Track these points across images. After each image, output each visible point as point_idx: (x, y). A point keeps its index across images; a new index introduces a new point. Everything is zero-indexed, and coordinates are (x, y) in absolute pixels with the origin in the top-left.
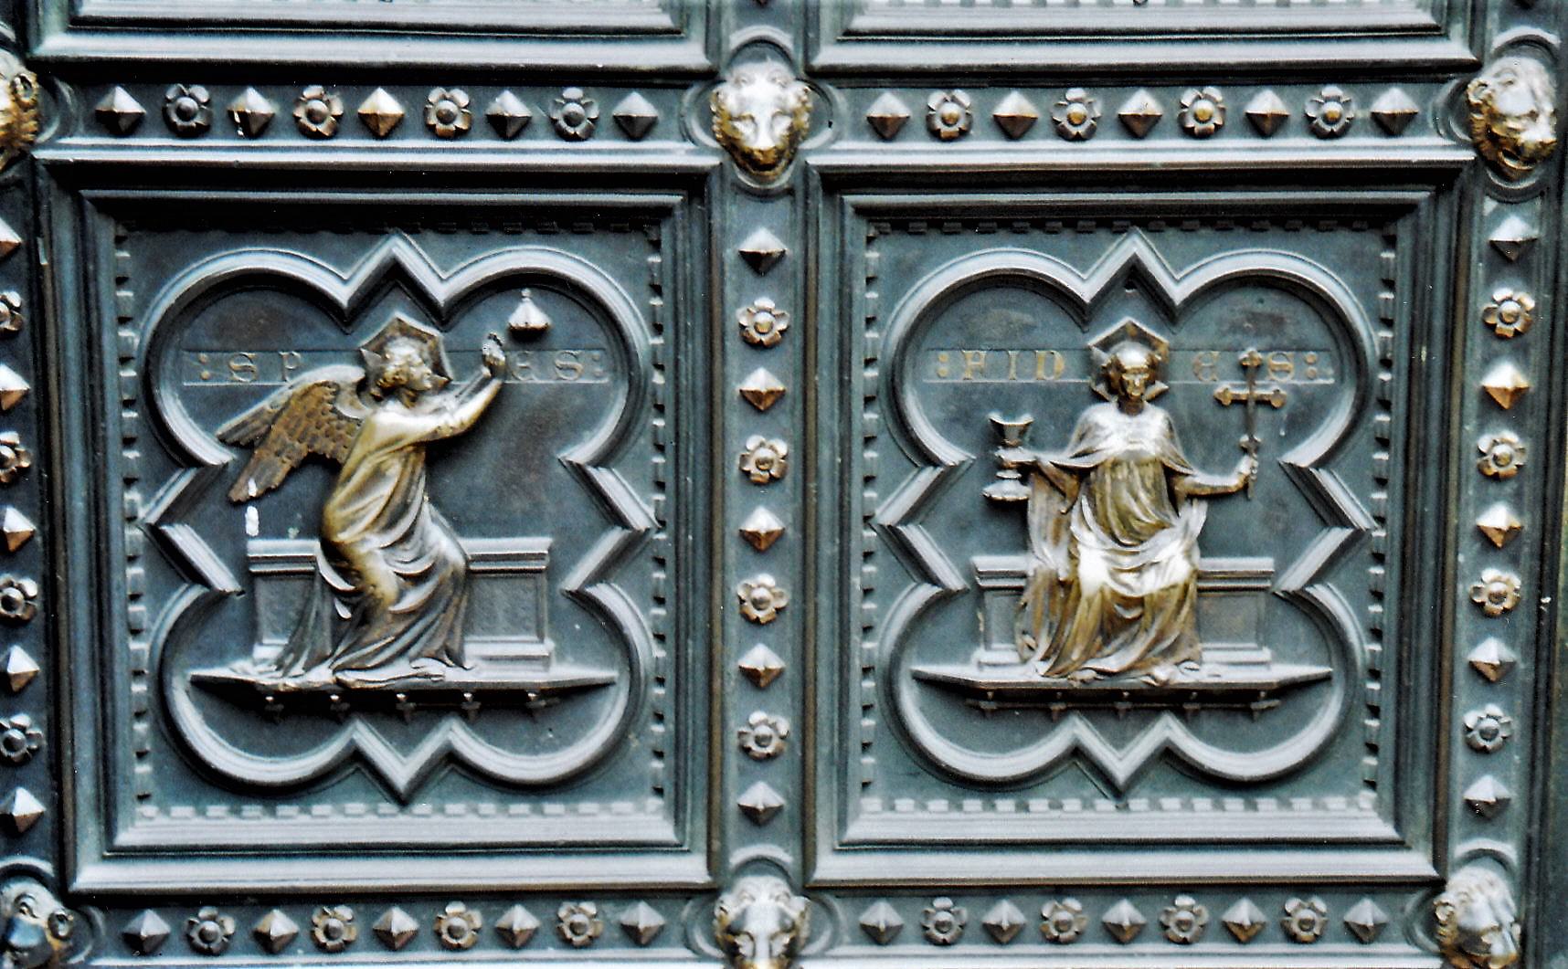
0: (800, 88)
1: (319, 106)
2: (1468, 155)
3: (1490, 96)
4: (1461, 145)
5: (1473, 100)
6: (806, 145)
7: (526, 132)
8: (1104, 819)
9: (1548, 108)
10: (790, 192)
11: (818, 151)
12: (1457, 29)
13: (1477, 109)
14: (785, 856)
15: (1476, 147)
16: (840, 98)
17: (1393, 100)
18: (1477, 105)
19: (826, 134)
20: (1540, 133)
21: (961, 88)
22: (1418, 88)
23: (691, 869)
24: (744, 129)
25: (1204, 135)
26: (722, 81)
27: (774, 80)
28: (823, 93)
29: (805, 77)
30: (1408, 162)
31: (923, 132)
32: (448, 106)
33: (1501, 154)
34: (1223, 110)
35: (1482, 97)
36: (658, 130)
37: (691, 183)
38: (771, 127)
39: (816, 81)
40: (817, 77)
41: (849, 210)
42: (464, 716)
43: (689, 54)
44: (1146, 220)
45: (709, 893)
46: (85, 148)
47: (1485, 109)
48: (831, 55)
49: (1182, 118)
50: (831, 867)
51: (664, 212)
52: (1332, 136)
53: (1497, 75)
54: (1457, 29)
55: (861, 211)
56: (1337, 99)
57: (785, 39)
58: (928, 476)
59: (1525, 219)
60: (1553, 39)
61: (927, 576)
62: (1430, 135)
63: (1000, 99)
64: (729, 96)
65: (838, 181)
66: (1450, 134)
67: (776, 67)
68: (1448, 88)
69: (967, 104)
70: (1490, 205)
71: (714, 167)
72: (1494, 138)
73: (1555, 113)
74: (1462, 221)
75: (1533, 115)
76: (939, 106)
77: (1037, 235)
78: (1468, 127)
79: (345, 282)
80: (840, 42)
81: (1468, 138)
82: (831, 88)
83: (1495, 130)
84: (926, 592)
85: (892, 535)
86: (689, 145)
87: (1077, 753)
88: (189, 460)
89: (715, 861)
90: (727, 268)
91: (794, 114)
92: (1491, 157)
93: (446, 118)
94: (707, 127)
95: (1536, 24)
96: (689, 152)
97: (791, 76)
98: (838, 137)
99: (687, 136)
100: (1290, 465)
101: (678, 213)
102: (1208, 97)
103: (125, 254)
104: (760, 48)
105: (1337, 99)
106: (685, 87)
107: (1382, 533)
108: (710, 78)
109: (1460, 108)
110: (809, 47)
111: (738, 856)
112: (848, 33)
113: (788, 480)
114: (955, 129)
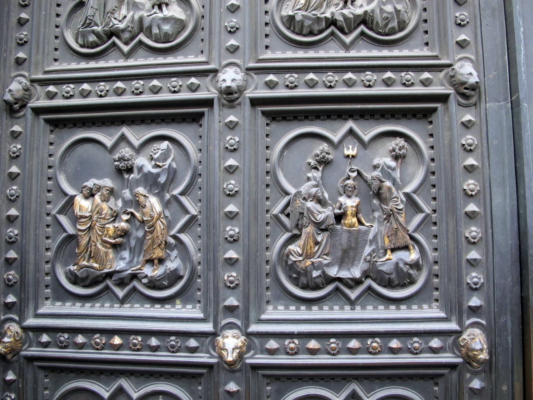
0: (243, 338)
1: (98, 340)
2: (460, 360)
3: (467, 343)
4: (458, 357)
5: (462, 344)
6: (246, 356)
7: (159, 349)
9: (485, 347)
10: (240, 370)
11: (248, 358)
12: (454, 318)
13: (463, 347)
15: (463, 358)
16: (256, 340)
17: (435, 343)
18: (463, 345)
19: (252, 352)
20: (484, 356)
21: (296, 338)
22: (442, 338)
24: (225, 353)
25: (375, 354)
26: (219, 335)
27: (234, 337)
28: (251, 340)
29: (245, 334)
30: (442, 362)
31: (283, 352)
32: (135, 341)
33: (471, 361)
34: (381, 346)
35: (464, 343)
36: (199, 350)
38: (233, 353)
40: (249, 335)
41: (260, 376)
43: (208, 327)
44: (357, 378)
46: (35, 351)
47: (466, 347)
48: (254, 328)
49: (368, 348)
52: (417, 354)
53: (469, 336)
54: (454, 318)
55: (264, 376)
56: (418, 342)
57: (239, 323)
59: (480, 380)
60: (484, 322)
62: (447, 352)
63: (309, 342)
66: (454, 353)
67: (236, 331)
68: (452, 338)
69: (297, 343)
70: (468, 375)
71: (215, 363)
72: (469, 357)
73: (488, 348)
74: (460, 380)
75: (481, 350)
76: (288, 344)
77: (322, 382)
78: (460, 351)
79: (108, 391)
80: (258, 323)
81: (460, 354)
82: (253, 338)
83: (470, 354)
86: (208, 355)
90: (220, 395)
91: (241, 347)
92: (468, 361)
93: (135, 345)
94: (214, 350)
95: (478, 318)
96: (208, 357)
97: (240, 335)
98: (255, 354)
99: (208, 352)
101: (205, 375)
102: (376, 342)
103: (48, 380)
104: (231, 326)
105: (418, 342)
106: (207, 337)
108: (214, 335)
109: (456, 347)
110: (247, 326)
112: (259, 320)
114: (294, 352)
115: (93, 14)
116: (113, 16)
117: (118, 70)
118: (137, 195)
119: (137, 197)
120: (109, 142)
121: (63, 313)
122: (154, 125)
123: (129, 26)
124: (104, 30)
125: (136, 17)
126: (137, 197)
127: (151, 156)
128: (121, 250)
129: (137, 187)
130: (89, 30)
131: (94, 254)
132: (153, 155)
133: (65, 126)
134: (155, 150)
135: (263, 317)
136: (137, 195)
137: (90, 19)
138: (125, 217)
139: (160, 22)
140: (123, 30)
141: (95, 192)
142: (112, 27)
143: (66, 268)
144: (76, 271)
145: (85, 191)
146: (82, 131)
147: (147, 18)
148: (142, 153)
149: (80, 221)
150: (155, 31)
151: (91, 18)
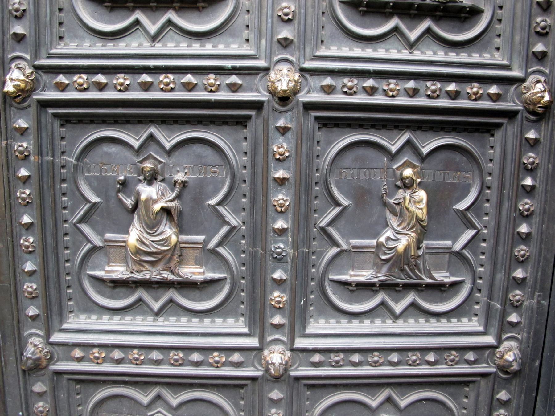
8: (390, 326)
11: (302, 96)
14: (284, 339)
23: (254, 342)
37: (257, 106)
39: (303, 73)
42: (176, 288)
45: (260, 350)
48: (309, 65)
50: (300, 343)
51: (249, 117)
55: (317, 118)
58: (338, 210)
61: (337, 245)
64: (273, 75)
65: (309, 107)
84: (334, 250)
85: (323, 229)
87: (383, 304)
88: (88, 201)
89: (262, 339)
100: (457, 209)
106: (258, 74)
107: (485, 231)
108: (267, 70)
111: (270, 338)
112: (314, 56)
113: (291, 211)
135: (318, 53)
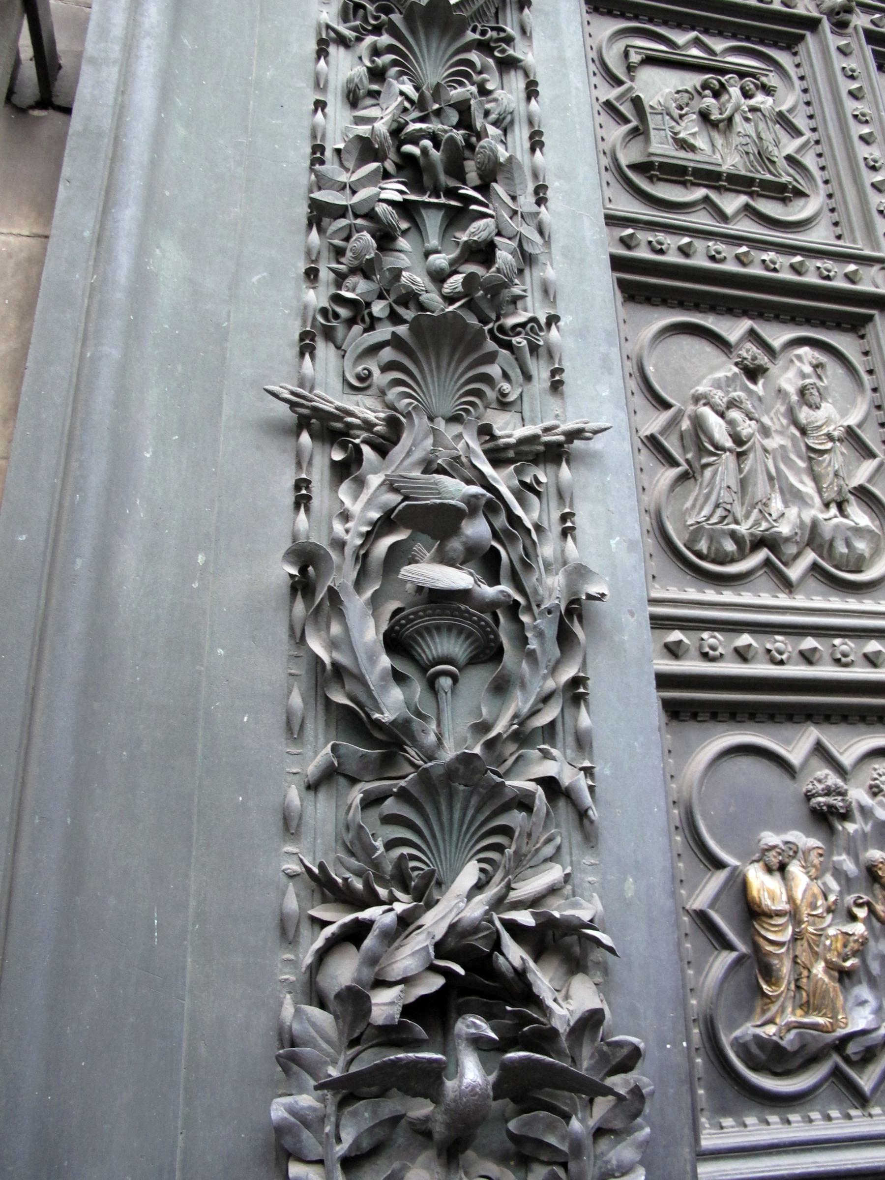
115: (731, 501)
116: (766, 509)
117: (792, 614)
118: (881, 865)
119: (880, 869)
120: (795, 754)
121: (762, 1143)
122: (862, 727)
123: (796, 533)
124: (752, 534)
125: (807, 519)
126: (880, 869)
127: (877, 786)
128: (853, 985)
129: (866, 849)
130: (723, 530)
131: (808, 995)
132: (882, 786)
133: (694, 716)
134: (880, 775)
136: (881, 865)
137: (726, 510)
138: (862, 913)
139: (849, 534)
140: (787, 540)
141: (786, 860)
142: (767, 530)
143: (731, 1033)
144: (774, 1038)
145: (775, 857)
146: (728, 730)
147: (825, 523)
148: (852, 781)
149: (773, 922)
150: (841, 549)
151: (728, 507)
